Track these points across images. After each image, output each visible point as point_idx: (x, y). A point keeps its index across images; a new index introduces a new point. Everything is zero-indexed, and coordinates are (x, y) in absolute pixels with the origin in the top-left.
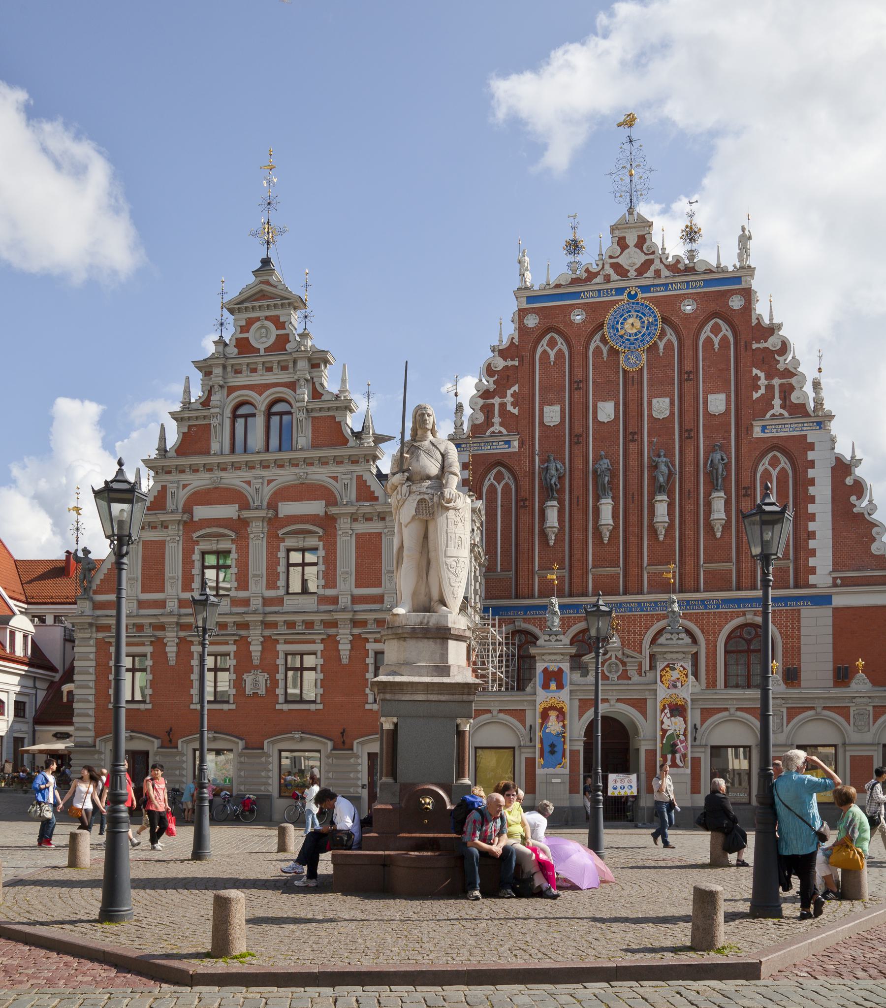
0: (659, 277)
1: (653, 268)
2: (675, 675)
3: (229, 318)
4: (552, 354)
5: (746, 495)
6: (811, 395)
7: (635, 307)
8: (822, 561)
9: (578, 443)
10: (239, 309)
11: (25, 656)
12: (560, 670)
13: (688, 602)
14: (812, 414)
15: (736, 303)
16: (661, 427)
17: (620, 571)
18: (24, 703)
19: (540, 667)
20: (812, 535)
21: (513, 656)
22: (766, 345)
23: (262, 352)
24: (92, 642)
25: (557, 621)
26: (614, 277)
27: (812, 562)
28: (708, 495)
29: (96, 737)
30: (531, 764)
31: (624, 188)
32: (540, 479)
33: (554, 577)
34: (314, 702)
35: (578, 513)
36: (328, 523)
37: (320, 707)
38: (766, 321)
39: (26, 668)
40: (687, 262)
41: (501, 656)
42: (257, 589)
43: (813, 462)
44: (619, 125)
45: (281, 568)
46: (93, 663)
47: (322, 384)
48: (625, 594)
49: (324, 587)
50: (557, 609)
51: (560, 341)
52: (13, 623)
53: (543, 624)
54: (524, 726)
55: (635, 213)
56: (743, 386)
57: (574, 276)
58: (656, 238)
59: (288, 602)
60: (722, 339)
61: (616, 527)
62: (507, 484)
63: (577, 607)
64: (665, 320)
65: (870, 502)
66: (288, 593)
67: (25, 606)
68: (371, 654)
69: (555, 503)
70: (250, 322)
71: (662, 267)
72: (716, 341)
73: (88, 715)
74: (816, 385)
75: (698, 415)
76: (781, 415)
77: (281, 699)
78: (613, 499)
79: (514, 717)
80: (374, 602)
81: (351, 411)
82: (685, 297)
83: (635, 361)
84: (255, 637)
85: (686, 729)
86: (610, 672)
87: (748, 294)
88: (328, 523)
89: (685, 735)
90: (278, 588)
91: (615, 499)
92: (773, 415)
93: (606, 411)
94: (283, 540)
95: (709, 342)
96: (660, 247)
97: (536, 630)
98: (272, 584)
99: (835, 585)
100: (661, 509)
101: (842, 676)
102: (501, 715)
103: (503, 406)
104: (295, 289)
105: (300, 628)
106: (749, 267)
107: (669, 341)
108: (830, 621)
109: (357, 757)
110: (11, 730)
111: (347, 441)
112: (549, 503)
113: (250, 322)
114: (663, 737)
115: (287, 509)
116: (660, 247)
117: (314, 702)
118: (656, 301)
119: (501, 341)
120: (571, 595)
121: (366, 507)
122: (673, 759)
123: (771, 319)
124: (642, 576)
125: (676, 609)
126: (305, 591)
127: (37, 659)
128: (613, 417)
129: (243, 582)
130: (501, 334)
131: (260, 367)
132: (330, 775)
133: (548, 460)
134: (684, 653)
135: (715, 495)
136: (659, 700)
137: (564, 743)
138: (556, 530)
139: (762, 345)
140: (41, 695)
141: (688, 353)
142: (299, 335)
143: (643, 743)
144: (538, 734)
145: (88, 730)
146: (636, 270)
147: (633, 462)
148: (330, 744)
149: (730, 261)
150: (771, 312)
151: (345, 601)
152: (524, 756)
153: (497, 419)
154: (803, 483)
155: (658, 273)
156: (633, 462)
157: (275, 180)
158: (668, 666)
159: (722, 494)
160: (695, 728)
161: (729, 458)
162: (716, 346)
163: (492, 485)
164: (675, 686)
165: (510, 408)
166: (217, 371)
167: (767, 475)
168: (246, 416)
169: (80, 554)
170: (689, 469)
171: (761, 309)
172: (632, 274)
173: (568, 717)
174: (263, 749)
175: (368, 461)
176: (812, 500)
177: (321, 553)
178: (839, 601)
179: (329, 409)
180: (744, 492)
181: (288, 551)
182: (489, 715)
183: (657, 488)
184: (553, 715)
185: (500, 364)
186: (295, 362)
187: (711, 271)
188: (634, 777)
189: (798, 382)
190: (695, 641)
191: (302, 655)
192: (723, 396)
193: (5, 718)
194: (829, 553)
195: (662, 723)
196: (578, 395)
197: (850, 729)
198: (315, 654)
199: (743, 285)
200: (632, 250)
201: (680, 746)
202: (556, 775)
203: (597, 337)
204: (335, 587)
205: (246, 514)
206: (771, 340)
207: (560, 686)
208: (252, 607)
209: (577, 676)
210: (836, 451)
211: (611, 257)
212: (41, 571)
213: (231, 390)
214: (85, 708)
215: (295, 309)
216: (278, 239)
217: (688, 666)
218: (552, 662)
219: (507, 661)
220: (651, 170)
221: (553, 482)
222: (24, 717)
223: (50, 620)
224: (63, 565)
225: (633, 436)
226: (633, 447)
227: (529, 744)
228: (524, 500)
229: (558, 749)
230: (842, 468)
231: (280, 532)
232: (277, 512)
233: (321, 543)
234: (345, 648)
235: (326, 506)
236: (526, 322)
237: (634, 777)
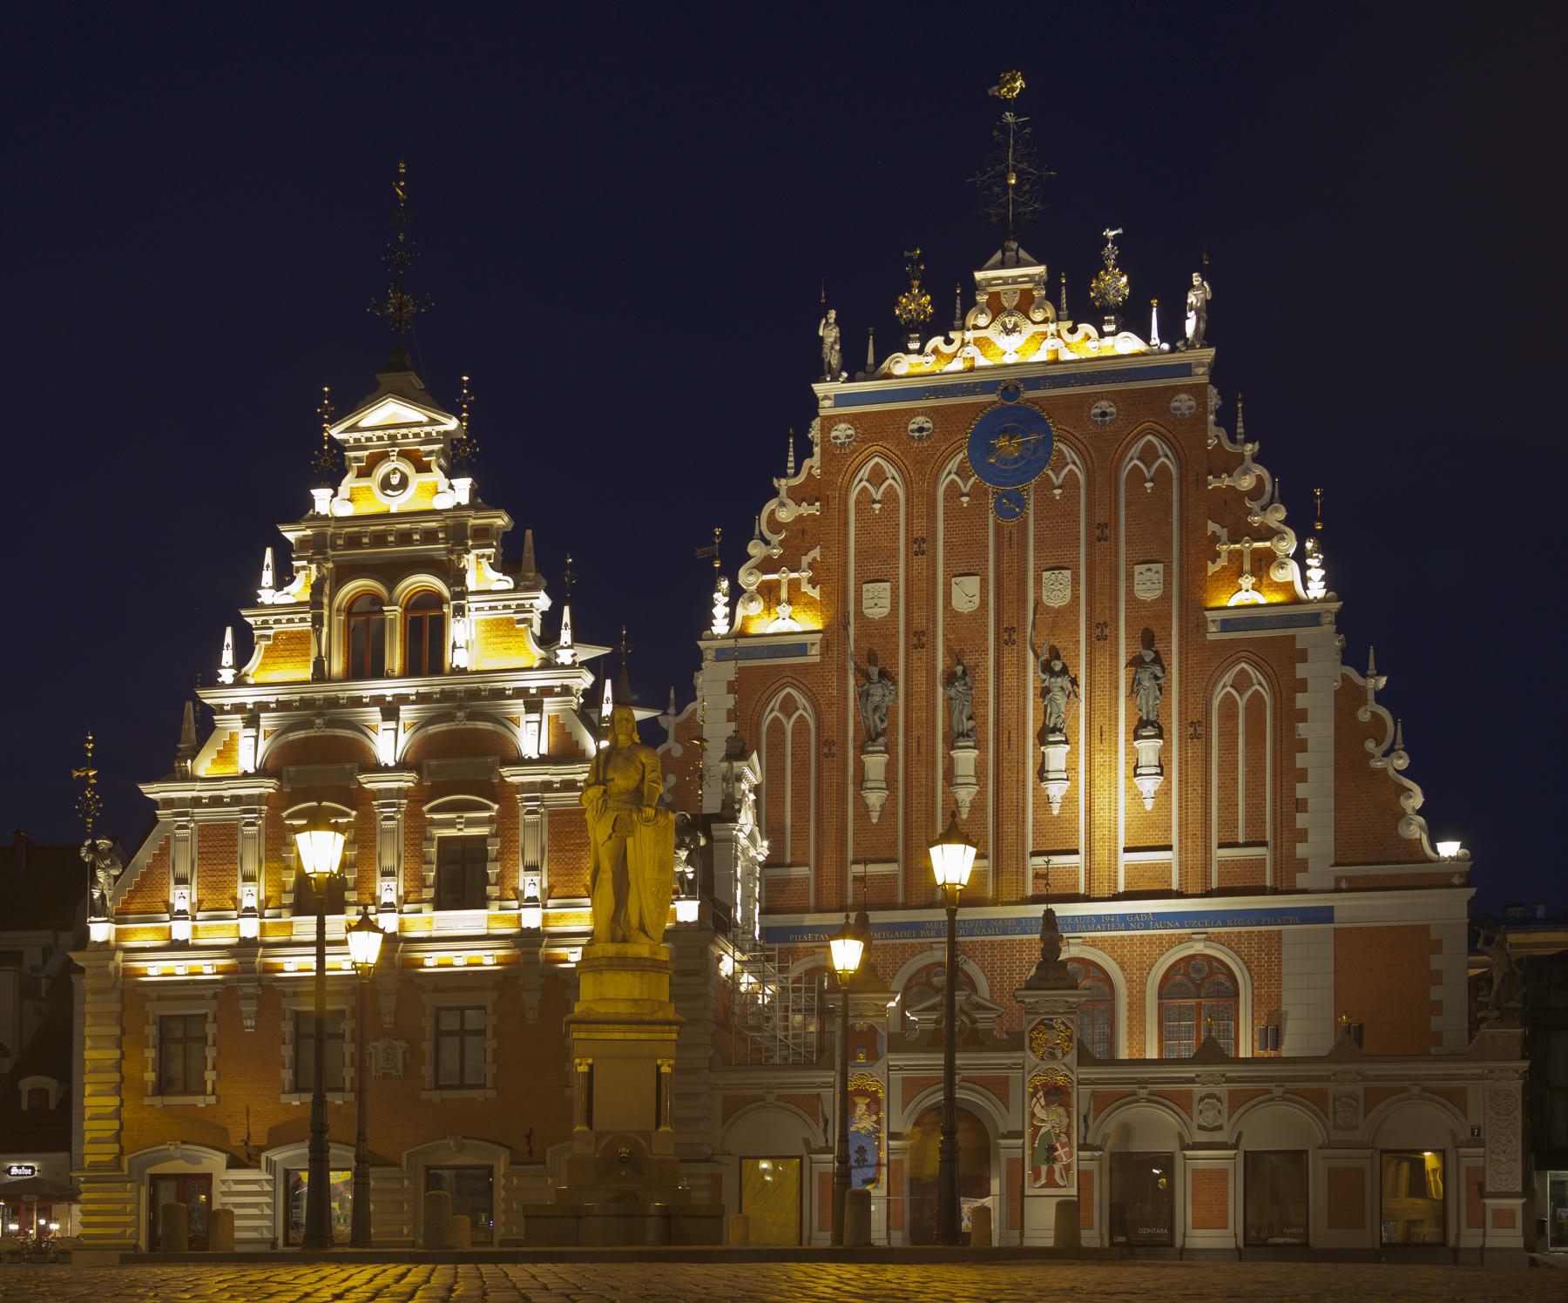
43: (1304, 682)
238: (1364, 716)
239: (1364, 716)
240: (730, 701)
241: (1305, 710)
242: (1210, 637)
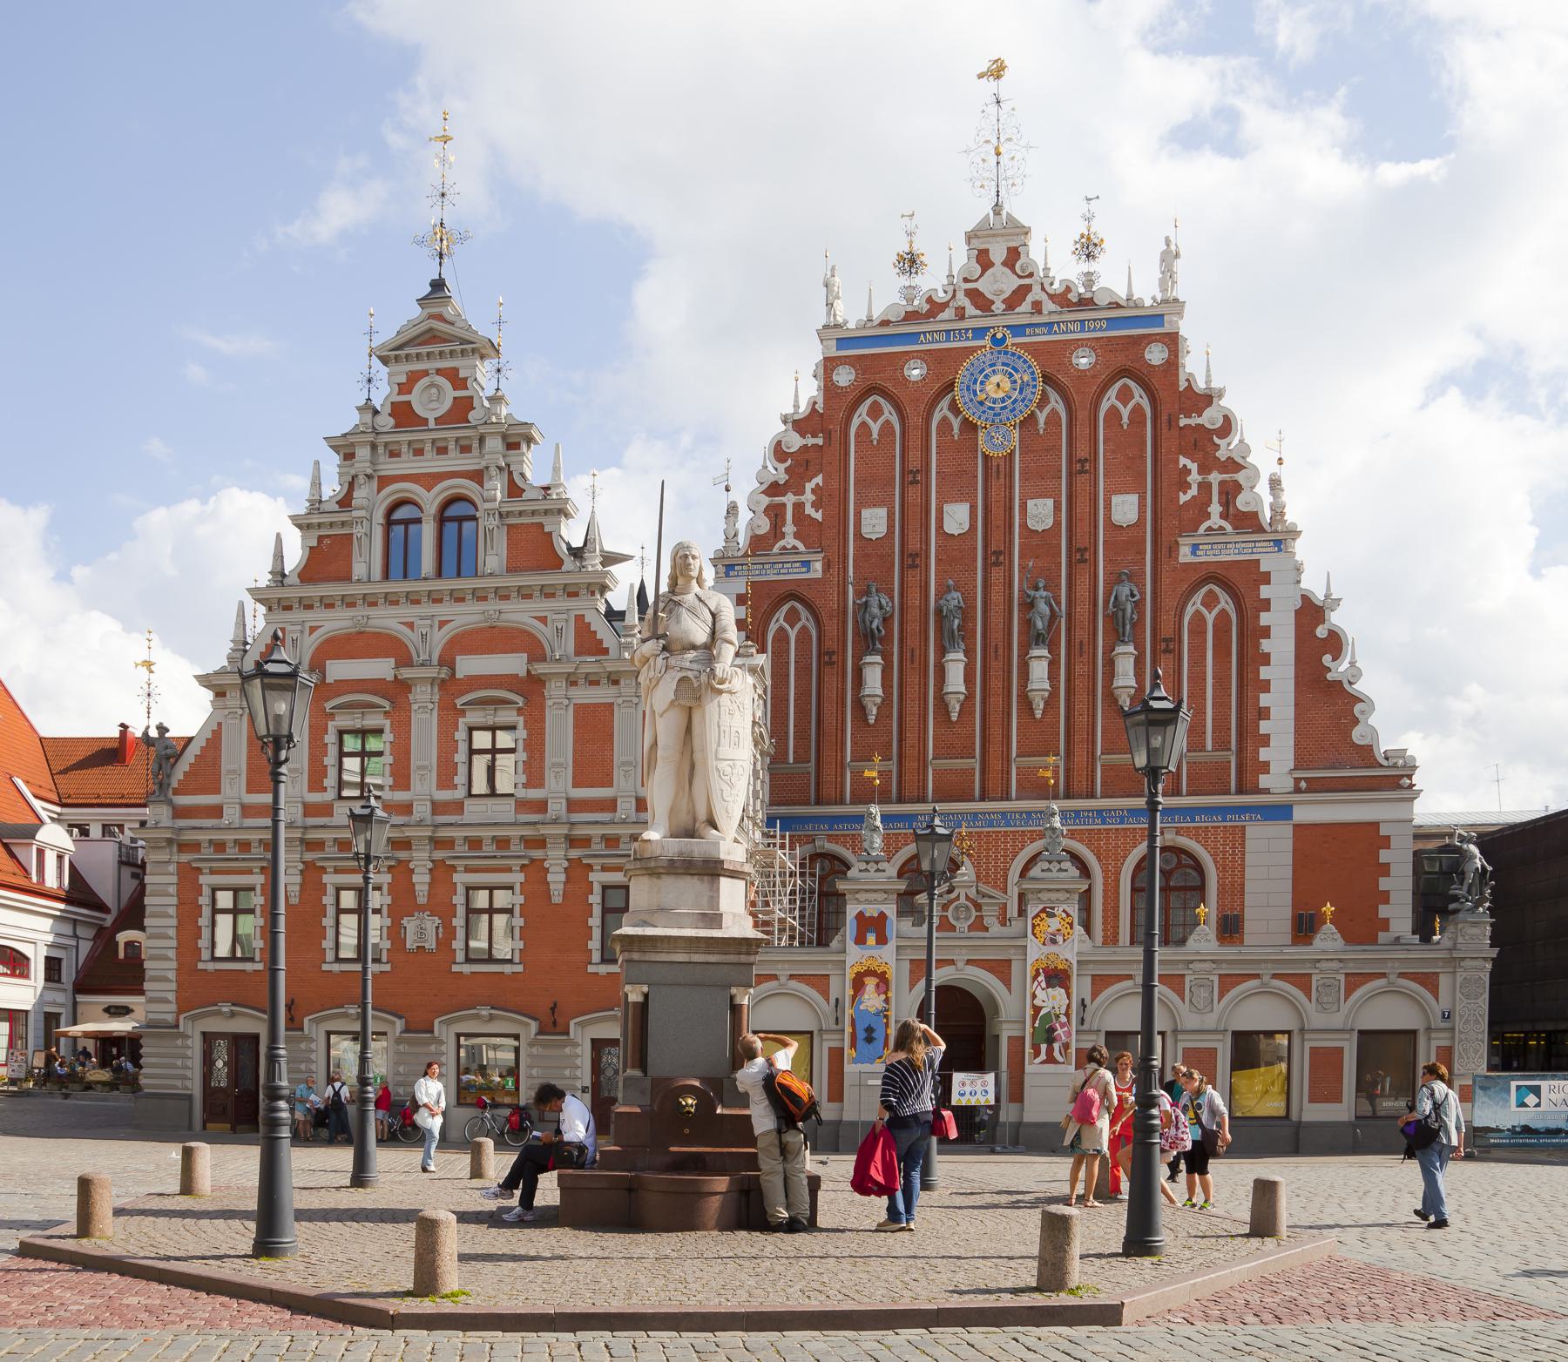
0: (1040, 312)
1: (1030, 298)
2: (1054, 924)
3: (381, 371)
4: (875, 428)
5: (1167, 651)
6: (1267, 499)
7: (1003, 358)
9: (914, 566)
10: (397, 358)
11: (60, 887)
12: (883, 916)
13: (1077, 812)
14: (1267, 528)
16: (1041, 543)
17: (976, 764)
18: (59, 960)
19: (852, 910)
20: (1264, 714)
21: (812, 892)
22: (1200, 421)
23: (432, 424)
24: (172, 868)
25: (878, 841)
26: (971, 310)
27: (1264, 754)
28: (1109, 649)
29: (179, 1012)
30: (837, 1056)
31: (987, 175)
32: (856, 622)
33: (875, 774)
34: (510, 961)
35: (912, 673)
36: (531, 688)
37: (520, 968)
38: (1200, 385)
39: (62, 906)
40: (1082, 290)
41: (793, 893)
42: (424, 787)
43: (1268, 601)
44: (981, 76)
45: (461, 757)
46: (174, 900)
47: (523, 475)
48: (982, 799)
49: (525, 786)
50: (878, 823)
51: (887, 407)
52: (43, 835)
53: (856, 843)
54: (828, 1000)
55: (1004, 213)
56: (1166, 482)
57: (910, 309)
58: (1035, 252)
59: (472, 808)
60: (1133, 411)
61: (970, 697)
62: (804, 628)
63: (908, 818)
64: (1048, 379)
65: (1352, 664)
66: (470, 795)
67: (58, 809)
68: (597, 889)
69: (878, 659)
70: (414, 377)
71: (1044, 297)
72: (1125, 413)
73: (166, 980)
74: (1275, 484)
75: (1096, 527)
76: (1221, 528)
77: (460, 956)
78: (966, 653)
79: (813, 986)
80: (602, 810)
81: (567, 515)
82: (1078, 344)
83: (999, 441)
84: (421, 861)
85: (1069, 1006)
86: (957, 919)
87: (1172, 341)
88: (531, 688)
89: (1067, 1014)
90: (455, 787)
91: (969, 653)
92: (1210, 529)
93: (957, 518)
94: (463, 713)
95: (1114, 413)
96: (1041, 267)
97: (847, 854)
98: (446, 781)
99: (1297, 790)
100: (1039, 671)
101: (1304, 927)
102: (793, 984)
103: (799, 507)
104: (481, 325)
105: (489, 849)
106: (1176, 300)
107: (1054, 411)
108: (1288, 845)
109: (576, 1045)
110: (41, 1001)
111: (561, 562)
112: (868, 659)
113: (414, 377)
114: (1034, 1018)
115: (468, 666)
116: (1041, 267)
117: (510, 961)
118: (1035, 350)
119: (796, 406)
120: (900, 800)
121: (590, 664)
122: (1050, 1051)
123: (1208, 382)
124: (1009, 772)
125: (1058, 825)
126: (493, 793)
127: (79, 893)
128: (966, 527)
129: (401, 778)
130: (796, 396)
131: (428, 447)
132: (534, 1072)
133: (867, 593)
134: (1067, 891)
135: (1120, 649)
136: (1029, 962)
137: (887, 1025)
138: (878, 700)
139: (1194, 421)
140: (85, 947)
141: (1082, 431)
142: (489, 399)
143: (1005, 1026)
144: (848, 1012)
145: (167, 1001)
146: (1004, 301)
147: (997, 597)
148: (534, 1026)
149: (1147, 292)
150: (1208, 370)
151: (557, 808)
152: (826, 1045)
153: (789, 528)
154: (1249, 636)
155: (1037, 306)
156: (997, 597)
157: (452, 159)
158: (1043, 910)
159: (1131, 648)
160: (1083, 1004)
161: (1143, 594)
162: (1125, 420)
163: (781, 629)
164: (1054, 942)
165: (809, 510)
166: (363, 453)
167: (1198, 619)
168: (406, 523)
169: (154, 733)
170: (1082, 610)
171: (1193, 367)
172: (998, 306)
173: (893, 986)
174: (432, 1031)
175: (593, 593)
176: (1266, 659)
177: (522, 733)
179: (534, 513)
180: (1163, 645)
181: (471, 730)
182: (773, 984)
183: (1033, 638)
184: (871, 983)
185: (795, 442)
186: (482, 440)
187: (1119, 306)
188: (990, 1077)
189: (1248, 478)
190: (1085, 871)
191: (491, 889)
192: (1134, 498)
193: (31, 982)
194: (1290, 741)
195: (1034, 996)
196: (914, 493)
197: (1310, 1007)
198: (511, 888)
199: (1167, 329)
200: (998, 270)
201: (1060, 1031)
202: (872, 1074)
203: (945, 403)
204: (541, 785)
205: (406, 673)
206: (1208, 413)
207: (882, 940)
208: (416, 816)
209: (906, 925)
210: (1302, 585)
211: (966, 280)
212: (81, 754)
213: (384, 481)
214: (161, 968)
215: (482, 357)
216: (456, 248)
217: (1074, 910)
218: (870, 902)
219: (803, 900)
220: (1028, 147)
221: (874, 626)
222: (59, 981)
223: (95, 831)
224: (116, 745)
225: (996, 557)
226: (997, 574)
227: (834, 1027)
228: (831, 654)
229: (879, 1035)
230: (1310, 612)
231: (459, 702)
232: (453, 669)
233: (521, 719)
234: (556, 879)
235: (530, 661)
236: (835, 378)
237: (990, 1077)
238: (1321, 632)
239: (1321, 632)
241: (1268, 628)
242: (1182, 560)
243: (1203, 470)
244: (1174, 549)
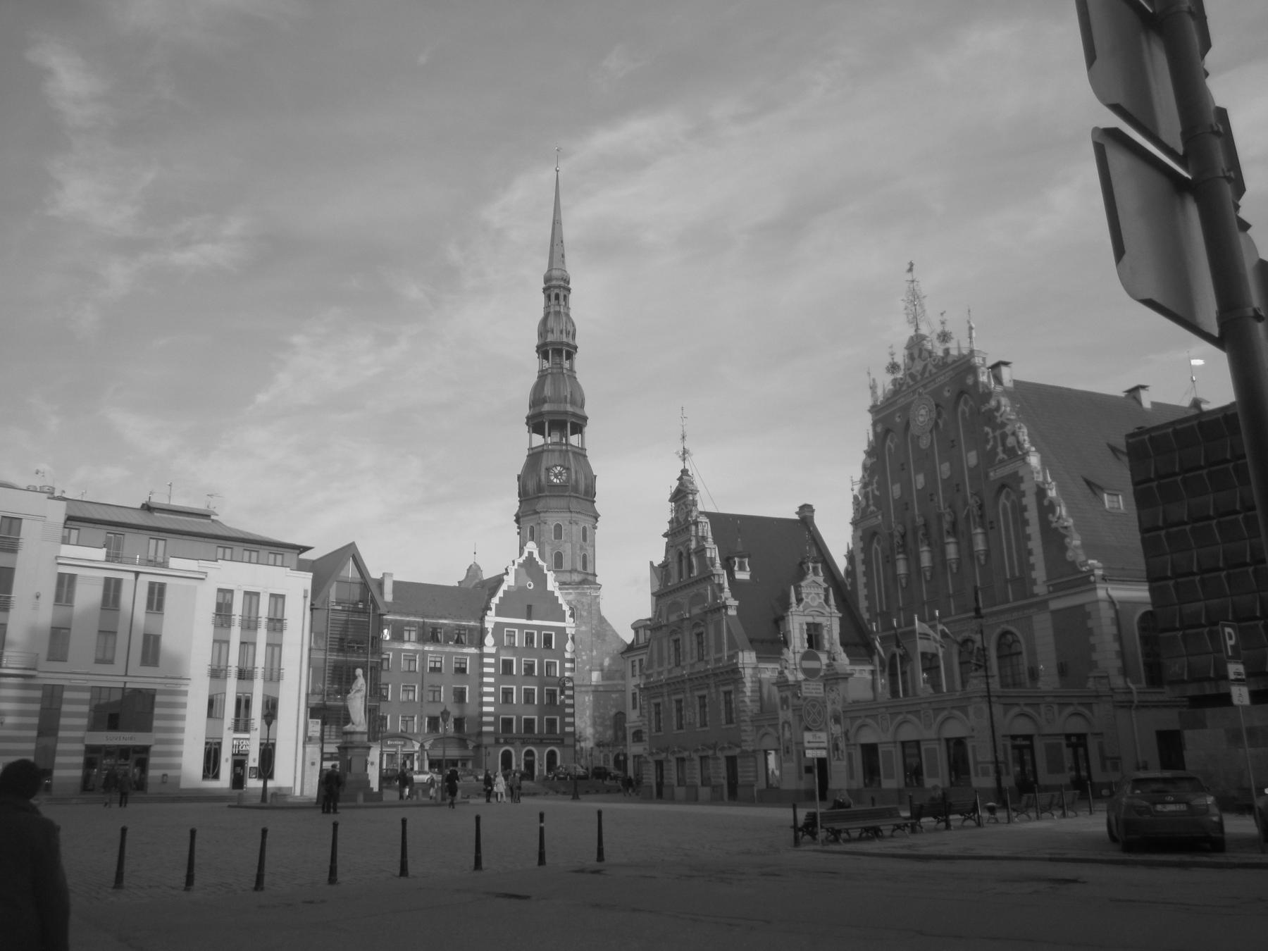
8: (1039, 574)
15: (970, 381)
83: (924, 443)
93: (920, 481)
95: (964, 413)
167: (1005, 505)
172: (919, 378)
178: (1054, 605)
200: (917, 361)
238: (1046, 503)
239: (1046, 503)
240: (861, 544)
243: (994, 430)
244: (987, 476)
